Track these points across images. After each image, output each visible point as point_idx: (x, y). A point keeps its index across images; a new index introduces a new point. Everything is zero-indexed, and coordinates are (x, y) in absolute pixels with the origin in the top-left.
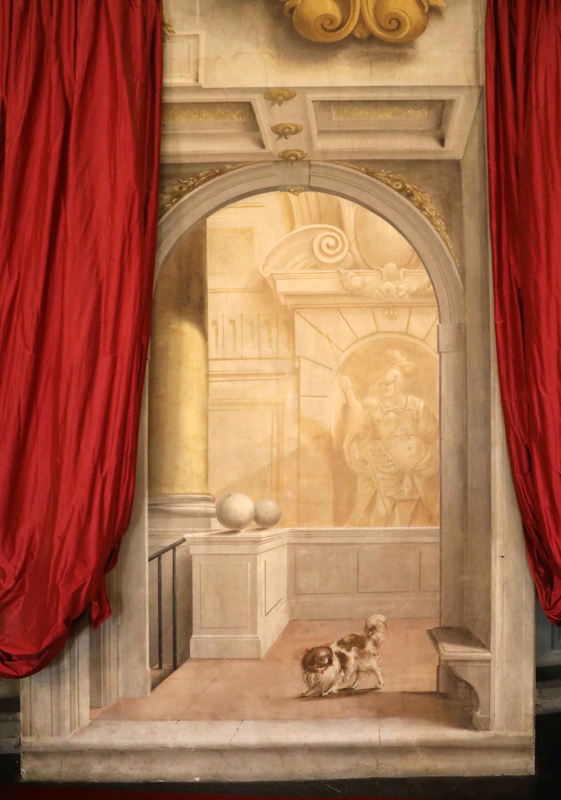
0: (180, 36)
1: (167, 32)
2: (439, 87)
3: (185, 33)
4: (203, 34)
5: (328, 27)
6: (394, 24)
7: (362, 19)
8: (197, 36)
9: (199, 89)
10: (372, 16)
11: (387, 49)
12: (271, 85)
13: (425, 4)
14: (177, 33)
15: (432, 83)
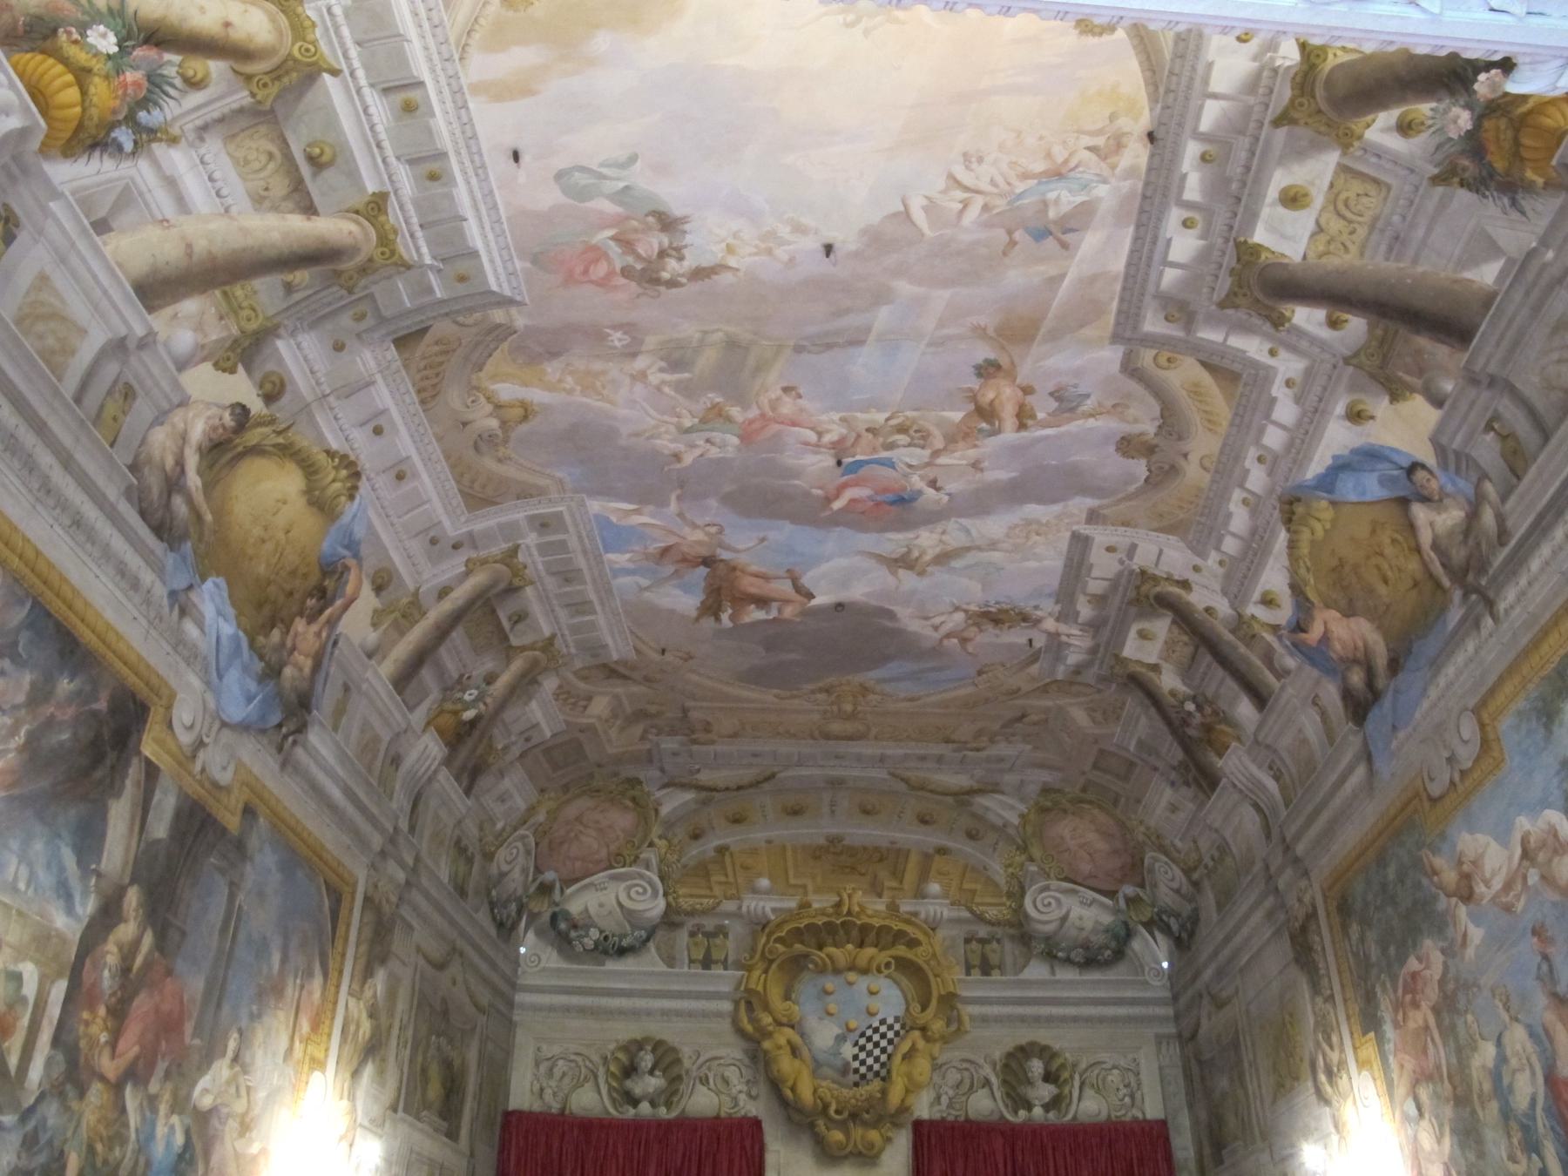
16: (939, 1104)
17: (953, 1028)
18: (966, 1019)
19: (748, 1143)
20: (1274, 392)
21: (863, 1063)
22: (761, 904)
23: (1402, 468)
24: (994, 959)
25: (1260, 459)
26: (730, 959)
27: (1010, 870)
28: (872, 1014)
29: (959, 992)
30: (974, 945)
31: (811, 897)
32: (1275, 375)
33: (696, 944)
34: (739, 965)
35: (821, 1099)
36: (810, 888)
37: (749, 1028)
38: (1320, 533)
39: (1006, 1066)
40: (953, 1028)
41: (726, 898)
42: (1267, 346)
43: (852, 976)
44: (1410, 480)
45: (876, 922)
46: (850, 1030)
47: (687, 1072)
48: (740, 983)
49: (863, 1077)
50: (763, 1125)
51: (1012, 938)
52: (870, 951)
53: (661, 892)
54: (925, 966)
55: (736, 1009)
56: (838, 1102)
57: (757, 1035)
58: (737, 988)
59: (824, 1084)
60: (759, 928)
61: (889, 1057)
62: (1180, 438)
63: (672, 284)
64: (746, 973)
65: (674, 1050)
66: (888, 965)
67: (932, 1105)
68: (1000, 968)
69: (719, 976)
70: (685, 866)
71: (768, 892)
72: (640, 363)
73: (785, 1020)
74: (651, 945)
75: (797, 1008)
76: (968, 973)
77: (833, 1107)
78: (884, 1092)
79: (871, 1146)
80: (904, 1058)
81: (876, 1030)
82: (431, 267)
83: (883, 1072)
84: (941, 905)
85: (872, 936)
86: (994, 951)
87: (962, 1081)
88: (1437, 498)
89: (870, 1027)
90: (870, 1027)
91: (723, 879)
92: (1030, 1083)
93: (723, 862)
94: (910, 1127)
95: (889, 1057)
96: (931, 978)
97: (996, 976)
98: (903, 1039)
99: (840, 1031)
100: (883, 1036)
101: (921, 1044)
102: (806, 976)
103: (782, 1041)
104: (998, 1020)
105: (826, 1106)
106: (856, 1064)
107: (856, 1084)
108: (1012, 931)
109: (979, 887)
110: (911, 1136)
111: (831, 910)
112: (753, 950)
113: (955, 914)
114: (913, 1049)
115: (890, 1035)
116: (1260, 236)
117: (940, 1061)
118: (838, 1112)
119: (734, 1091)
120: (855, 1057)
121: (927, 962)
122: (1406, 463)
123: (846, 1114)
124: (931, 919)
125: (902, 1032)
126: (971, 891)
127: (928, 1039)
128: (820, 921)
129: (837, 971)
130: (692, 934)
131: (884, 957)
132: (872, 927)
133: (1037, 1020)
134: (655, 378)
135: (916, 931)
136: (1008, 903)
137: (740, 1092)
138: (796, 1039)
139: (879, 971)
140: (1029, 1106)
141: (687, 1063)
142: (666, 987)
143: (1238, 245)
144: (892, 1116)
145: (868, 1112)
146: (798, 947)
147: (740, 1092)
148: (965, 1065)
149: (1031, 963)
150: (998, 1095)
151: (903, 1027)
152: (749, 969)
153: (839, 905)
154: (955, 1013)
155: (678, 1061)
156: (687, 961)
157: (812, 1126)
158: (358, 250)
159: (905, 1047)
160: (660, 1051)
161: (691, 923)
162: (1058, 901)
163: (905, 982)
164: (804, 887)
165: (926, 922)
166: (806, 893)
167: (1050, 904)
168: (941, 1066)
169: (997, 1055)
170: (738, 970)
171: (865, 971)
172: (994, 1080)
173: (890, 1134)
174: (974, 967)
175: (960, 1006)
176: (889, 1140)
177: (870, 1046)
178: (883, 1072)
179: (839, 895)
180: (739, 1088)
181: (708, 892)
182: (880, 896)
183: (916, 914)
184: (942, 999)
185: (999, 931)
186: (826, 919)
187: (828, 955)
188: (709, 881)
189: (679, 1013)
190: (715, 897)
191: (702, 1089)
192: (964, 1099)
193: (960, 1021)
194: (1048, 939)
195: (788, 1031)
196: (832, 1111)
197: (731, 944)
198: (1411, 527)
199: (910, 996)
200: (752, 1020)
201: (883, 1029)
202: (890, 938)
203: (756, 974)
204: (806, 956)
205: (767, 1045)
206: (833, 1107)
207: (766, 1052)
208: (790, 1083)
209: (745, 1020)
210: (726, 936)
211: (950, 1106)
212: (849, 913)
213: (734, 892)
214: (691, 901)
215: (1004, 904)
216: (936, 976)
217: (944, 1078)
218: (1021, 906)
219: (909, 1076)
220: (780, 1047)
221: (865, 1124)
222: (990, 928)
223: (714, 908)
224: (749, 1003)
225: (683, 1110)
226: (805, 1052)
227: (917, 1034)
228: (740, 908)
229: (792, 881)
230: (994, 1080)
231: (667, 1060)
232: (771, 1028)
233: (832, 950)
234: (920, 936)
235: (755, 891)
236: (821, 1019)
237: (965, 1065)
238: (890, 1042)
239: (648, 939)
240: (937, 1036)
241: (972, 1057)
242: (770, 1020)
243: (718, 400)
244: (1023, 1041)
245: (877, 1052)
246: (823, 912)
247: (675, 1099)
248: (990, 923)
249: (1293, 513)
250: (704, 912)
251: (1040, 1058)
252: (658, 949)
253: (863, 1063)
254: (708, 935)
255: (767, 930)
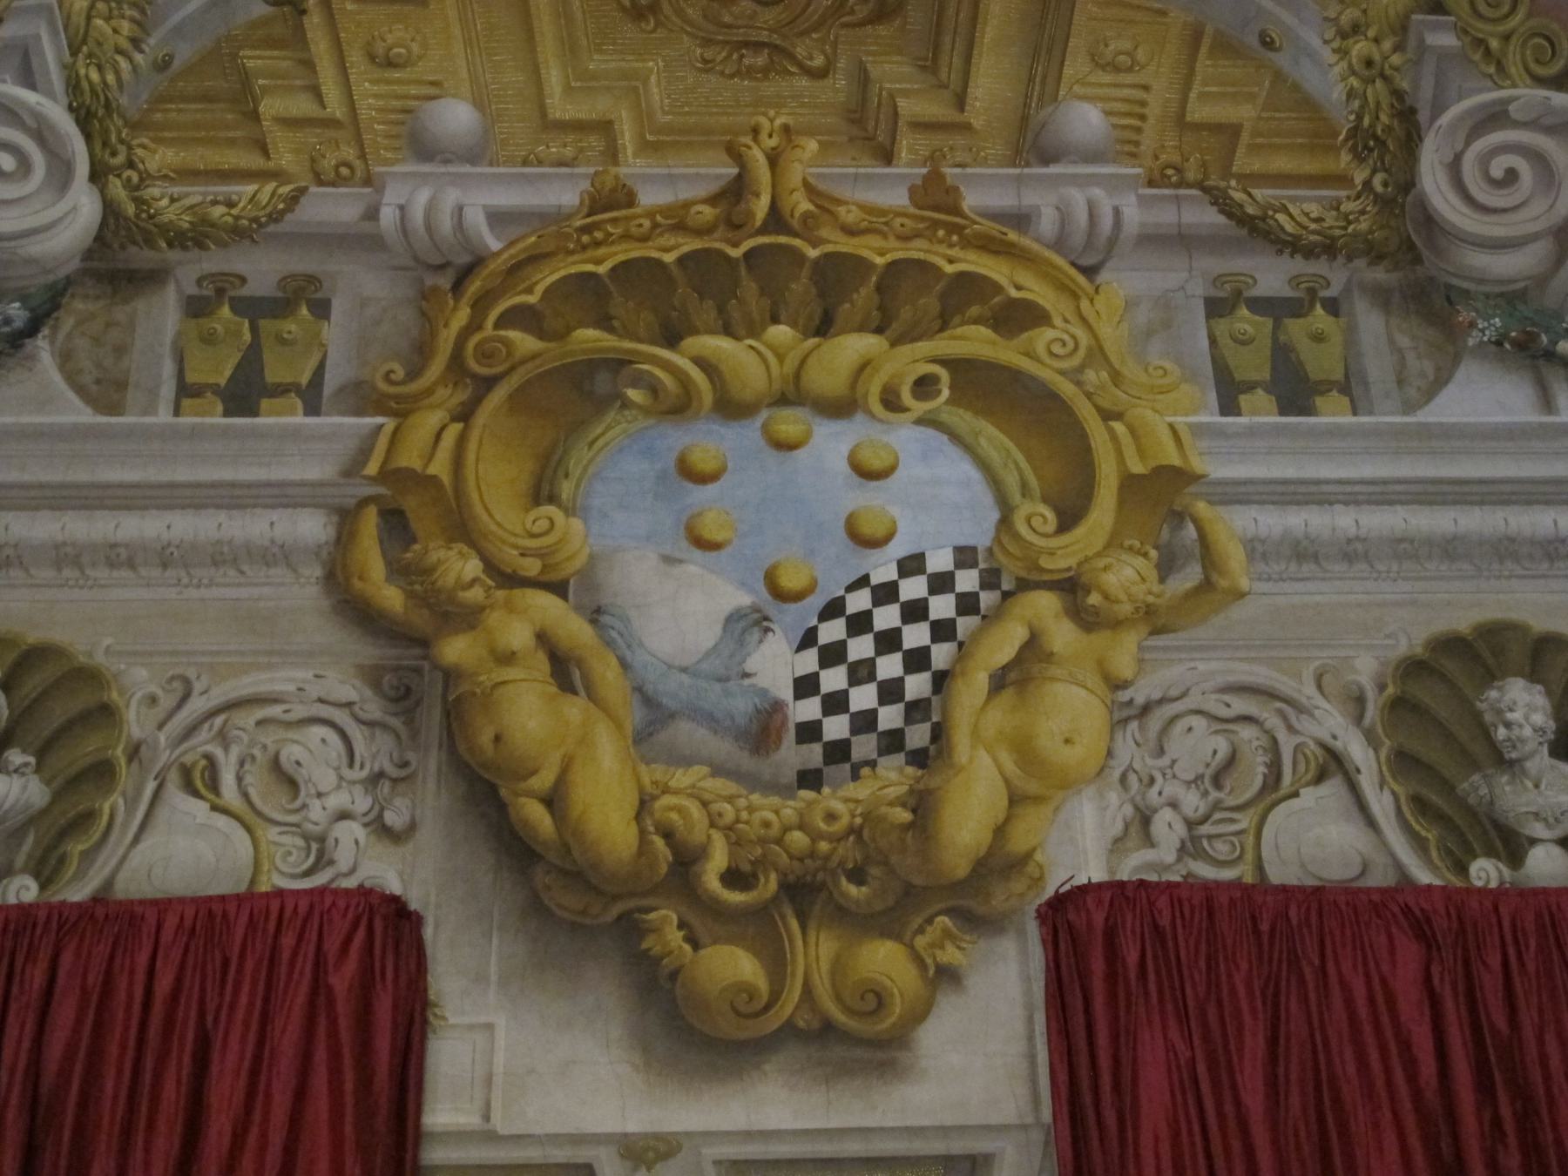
0: (453, 1026)
1: (431, 1018)
2: (962, 1129)
3: (466, 1020)
4: (501, 1022)
5: (743, 1009)
6: (871, 1002)
7: (807, 989)
8: (489, 1027)
9: (491, 1137)
10: (827, 986)
11: (859, 1053)
12: (632, 1127)
13: (929, 961)
14: (452, 1021)
15: (949, 1120)
16: (1149, 841)
17: (1190, 576)
18: (1234, 556)
19: (341, 981)
21: (835, 703)
22: (451, 197)
24: (1321, 362)
26: (330, 383)
27: (1360, 48)
28: (863, 539)
29: (1198, 464)
30: (1245, 321)
31: (633, 166)
33: (209, 339)
34: (361, 398)
35: (668, 835)
36: (627, 137)
37: (391, 597)
39: (1401, 707)
40: (1190, 576)
41: (321, 183)
43: (789, 422)
45: (877, 252)
46: (781, 595)
47: (134, 752)
48: (364, 453)
49: (838, 752)
50: (428, 932)
51: (1382, 297)
52: (853, 346)
53: (82, 168)
54: (1067, 389)
55: (345, 536)
56: (736, 842)
57: (421, 620)
58: (352, 470)
59: (682, 778)
60: (445, 282)
61: (941, 680)
64: (389, 423)
65: (89, 676)
66: (924, 386)
67: (1118, 846)
68: (1345, 389)
69: (295, 434)
70: (163, 65)
71: (473, 157)
73: (532, 567)
74: (43, 348)
75: (576, 524)
76: (1229, 407)
77: (718, 860)
78: (922, 805)
79: (878, 999)
80: (999, 681)
81: (886, 594)
83: (918, 736)
84: (1114, 184)
85: (864, 296)
86: (1319, 338)
87: (1232, 760)
89: (863, 581)
90: (863, 581)
91: (302, 106)
92: (1502, 761)
93: (299, 38)
94: (1033, 929)
95: (941, 680)
96: (1086, 413)
97: (1333, 414)
98: (991, 619)
99: (744, 600)
100: (915, 612)
101: (1063, 635)
102: (613, 429)
103: (518, 636)
104: (1353, 552)
105: (686, 860)
106: (809, 709)
107: (810, 779)
108: (1379, 274)
109: (1244, 113)
110: (1037, 956)
111: (708, 213)
112: (422, 351)
113: (1166, 216)
114: (1033, 648)
115: (942, 607)
117: (1140, 694)
118: (733, 878)
119: (317, 813)
120: (805, 686)
121: (1075, 376)
123: (770, 885)
124: (1078, 238)
125: (987, 599)
126: (1217, 128)
127: (1086, 619)
128: (670, 251)
129: (731, 408)
130: (196, 308)
131: (912, 359)
132: (860, 265)
133: (1506, 550)
135: (1026, 278)
136: (1359, 177)
137: (344, 816)
138: (573, 628)
139: (891, 403)
140: (1512, 847)
141: (135, 722)
142: (81, 475)
144: (957, 887)
145: (857, 876)
146: (588, 336)
147: (344, 816)
148: (1240, 705)
149: (1461, 374)
150: (1381, 804)
151: (990, 580)
152: (401, 409)
153: (736, 191)
154: (1190, 531)
155: (105, 714)
156: (168, 390)
157: (630, 929)
159: (1004, 645)
160: (33, 684)
161: (190, 270)
162: (1538, 158)
163: (992, 437)
164: (605, 127)
165: (1059, 245)
166: (612, 154)
167: (1511, 176)
168: (1146, 709)
169: (1365, 669)
170: (359, 413)
171: (840, 408)
172: (1357, 750)
173: (950, 955)
174: (1250, 387)
175: (1201, 508)
176: (947, 976)
177: (861, 647)
178: (918, 736)
179: (735, 154)
180: (337, 801)
181: (253, 161)
182: (887, 157)
183: (1021, 220)
184: (1130, 485)
185: (1336, 276)
186: (690, 245)
187: (701, 362)
188: (255, 116)
189: (120, 557)
190: (277, 175)
191: (187, 808)
192: (1245, 821)
193: (1206, 551)
194: (1511, 298)
195: (544, 604)
196: (711, 877)
197: (336, 333)
199: (1011, 481)
200: (399, 571)
201: (913, 588)
202: (930, 303)
203: (431, 419)
204: (619, 364)
205: (456, 649)
206: (718, 860)
207: (450, 675)
208: (544, 780)
209: (376, 568)
210: (322, 309)
211: (1191, 847)
212: (777, 220)
213: (349, 153)
214: (195, 194)
215: (1343, 180)
216: (1107, 416)
217: (1161, 752)
218: (1408, 184)
219: (1025, 751)
220: (507, 658)
221: (847, 919)
222: (1299, 265)
223: (275, 217)
224: (396, 524)
225: (109, 884)
226: (608, 674)
227: (1045, 604)
228: (372, 214)
229: (560, 108)
230: (1357, 750)
231: (60, 711)
232: (475, 595)
233: (722, 344)
234: (1039, 292)
235: (424, 149)
236: (668, 560)
237: (1240, 705)
238: (943, 630)
239: (32, 329)
240: (1126, 609)
241: (1260, 674)
242: (473, 567)
244: (1463, 621)
245: (890, 666)
246: (677, 220)
247: (76, 847)
248: (1292, 246)
250: (241, 234)
251: (1534, 676)
252: (65, 359)
253: (835, 703)
254: (253, 309)
255: (474, 287)
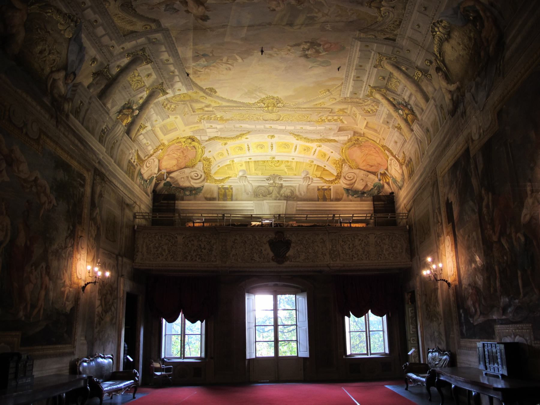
20: (113, 42)
23: (75, 70)
25: (96, 21)
32: (117, 45)
38: (60, 27)
42: (126, 48)
44: (71, 73)
62: (122, 5)
63: (306, 42)
72: (324, 19)
82: (374, 51)
88: (66, 82)
116: (149, 66)
122: (76, 72)
134: (320, 15)
143: (152, 62)
158: (387, 62)
198: (58, 70)
243: (299, 7)
249: (72, 21)
